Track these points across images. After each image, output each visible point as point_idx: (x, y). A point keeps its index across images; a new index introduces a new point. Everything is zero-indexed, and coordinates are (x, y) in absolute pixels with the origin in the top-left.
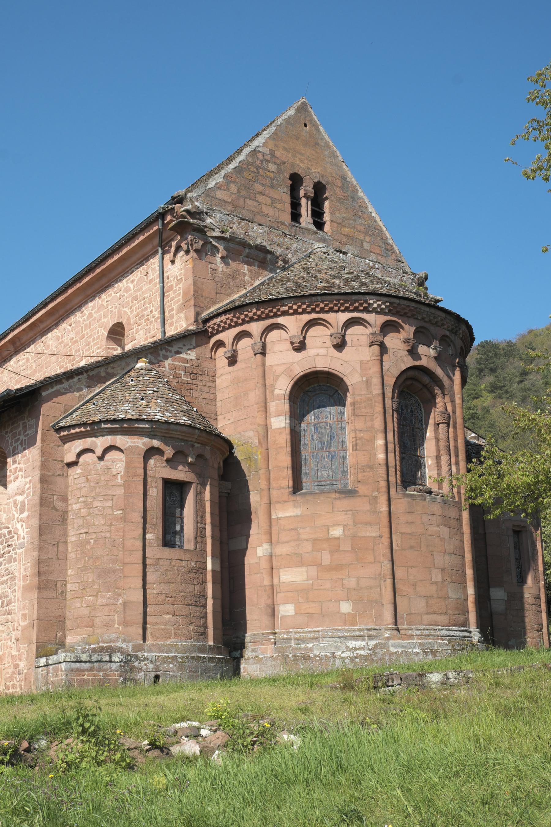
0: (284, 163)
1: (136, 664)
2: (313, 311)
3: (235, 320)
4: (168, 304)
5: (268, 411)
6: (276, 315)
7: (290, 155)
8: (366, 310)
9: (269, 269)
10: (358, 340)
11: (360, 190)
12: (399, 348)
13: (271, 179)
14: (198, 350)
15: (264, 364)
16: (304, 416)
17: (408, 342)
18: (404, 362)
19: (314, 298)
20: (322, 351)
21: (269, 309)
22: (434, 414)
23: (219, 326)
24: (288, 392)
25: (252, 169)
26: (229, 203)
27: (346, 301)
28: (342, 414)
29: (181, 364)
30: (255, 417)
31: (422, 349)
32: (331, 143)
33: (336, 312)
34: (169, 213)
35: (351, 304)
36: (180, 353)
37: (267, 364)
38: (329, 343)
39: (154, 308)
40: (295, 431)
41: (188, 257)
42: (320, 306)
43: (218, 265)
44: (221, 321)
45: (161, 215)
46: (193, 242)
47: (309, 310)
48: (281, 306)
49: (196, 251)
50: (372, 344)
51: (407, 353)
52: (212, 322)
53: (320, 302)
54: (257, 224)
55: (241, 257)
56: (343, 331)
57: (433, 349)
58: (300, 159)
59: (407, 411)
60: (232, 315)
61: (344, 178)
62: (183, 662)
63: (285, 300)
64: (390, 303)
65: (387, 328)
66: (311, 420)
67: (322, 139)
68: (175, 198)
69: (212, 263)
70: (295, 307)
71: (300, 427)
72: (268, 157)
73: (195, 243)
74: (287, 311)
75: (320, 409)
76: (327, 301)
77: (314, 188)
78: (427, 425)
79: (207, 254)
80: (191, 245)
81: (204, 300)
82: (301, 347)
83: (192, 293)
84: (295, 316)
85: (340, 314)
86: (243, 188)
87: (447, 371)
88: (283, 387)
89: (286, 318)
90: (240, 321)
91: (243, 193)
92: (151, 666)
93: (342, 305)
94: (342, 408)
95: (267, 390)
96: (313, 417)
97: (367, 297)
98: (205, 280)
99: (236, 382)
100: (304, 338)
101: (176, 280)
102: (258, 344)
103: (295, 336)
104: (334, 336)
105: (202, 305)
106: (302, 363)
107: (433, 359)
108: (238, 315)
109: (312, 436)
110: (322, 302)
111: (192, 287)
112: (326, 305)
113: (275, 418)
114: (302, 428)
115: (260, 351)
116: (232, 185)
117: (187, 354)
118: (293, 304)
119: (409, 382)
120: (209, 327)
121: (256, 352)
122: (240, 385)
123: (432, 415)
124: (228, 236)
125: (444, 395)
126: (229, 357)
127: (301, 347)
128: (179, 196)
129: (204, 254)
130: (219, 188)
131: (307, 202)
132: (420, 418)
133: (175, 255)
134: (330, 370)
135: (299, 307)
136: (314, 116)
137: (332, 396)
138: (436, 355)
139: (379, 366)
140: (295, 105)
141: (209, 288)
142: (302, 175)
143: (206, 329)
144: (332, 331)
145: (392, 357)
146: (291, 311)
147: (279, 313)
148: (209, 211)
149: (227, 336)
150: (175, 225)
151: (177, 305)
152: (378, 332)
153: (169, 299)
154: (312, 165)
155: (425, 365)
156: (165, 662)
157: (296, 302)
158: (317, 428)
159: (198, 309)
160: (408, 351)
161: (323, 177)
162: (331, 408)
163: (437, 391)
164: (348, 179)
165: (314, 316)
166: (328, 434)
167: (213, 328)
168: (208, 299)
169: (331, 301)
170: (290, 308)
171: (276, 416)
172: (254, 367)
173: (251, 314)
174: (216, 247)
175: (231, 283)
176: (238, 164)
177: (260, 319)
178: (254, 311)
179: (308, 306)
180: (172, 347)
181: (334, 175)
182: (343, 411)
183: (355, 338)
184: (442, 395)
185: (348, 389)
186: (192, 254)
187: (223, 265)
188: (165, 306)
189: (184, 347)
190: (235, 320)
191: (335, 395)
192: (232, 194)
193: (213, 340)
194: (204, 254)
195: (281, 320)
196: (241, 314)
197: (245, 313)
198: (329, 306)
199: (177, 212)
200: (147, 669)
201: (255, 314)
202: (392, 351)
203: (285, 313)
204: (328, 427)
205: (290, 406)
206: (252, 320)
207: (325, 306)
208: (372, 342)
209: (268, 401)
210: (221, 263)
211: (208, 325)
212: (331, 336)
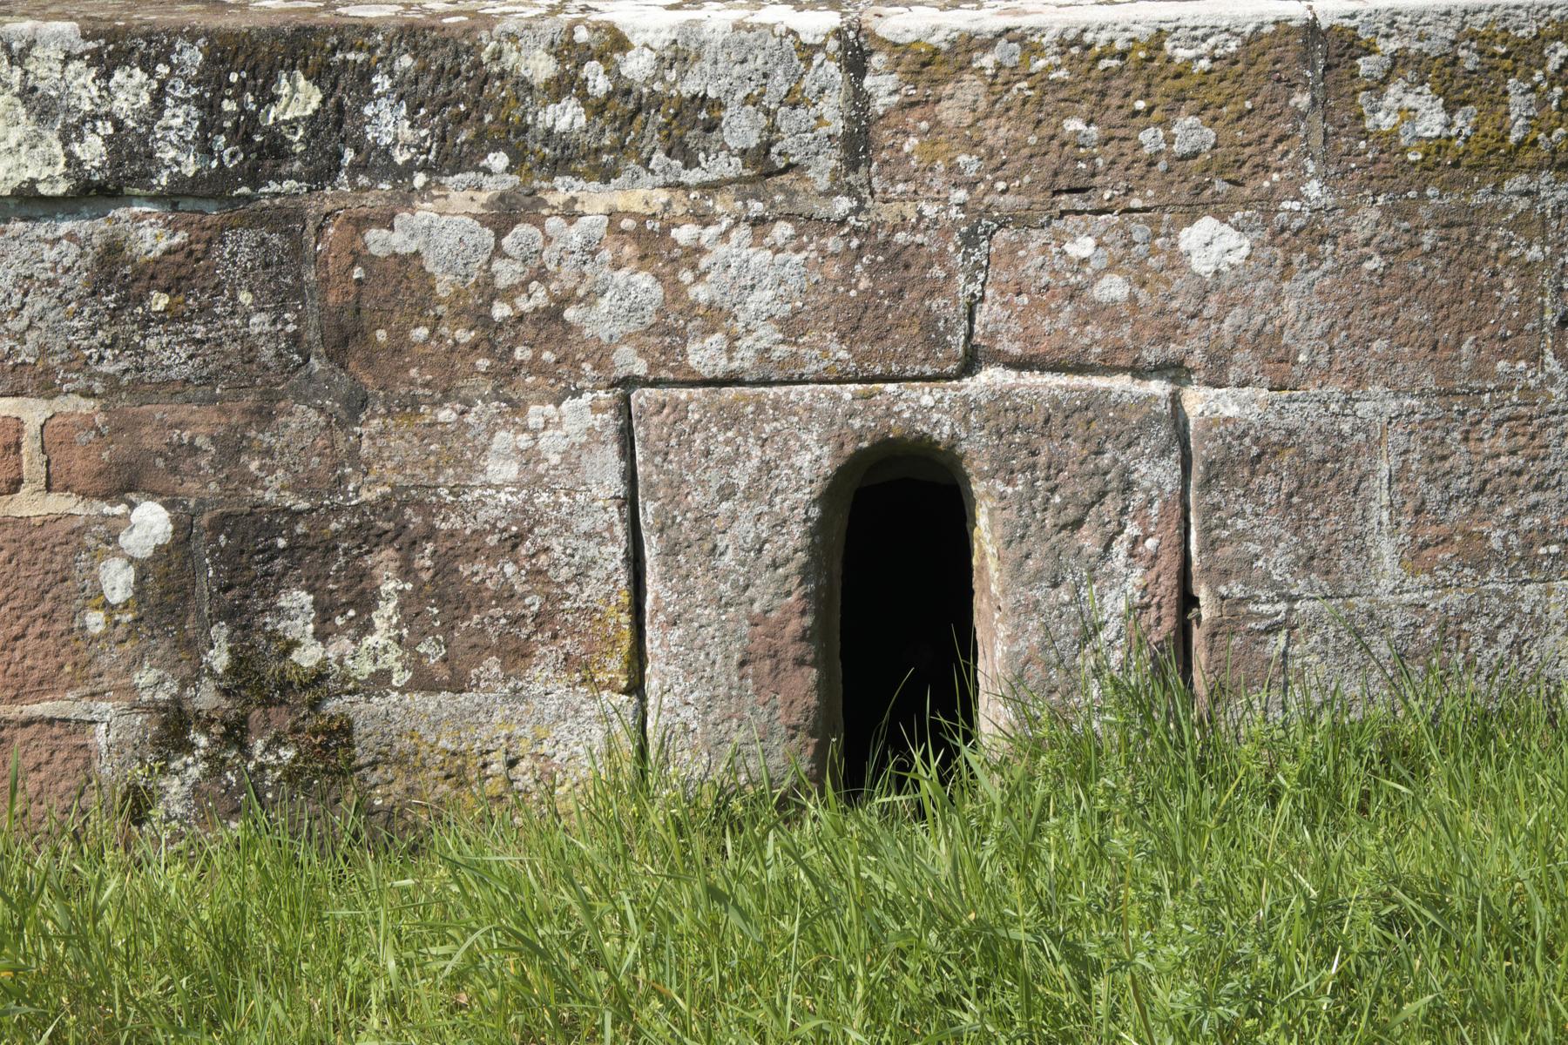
1: (441, 227)
62: (1497, 157)
92: (755, 273)
156: (1070, 187)
200: (669, 329)
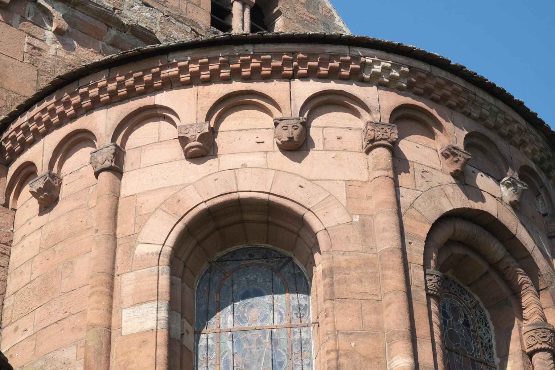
2: (236, 75)
3: (60, 109)
5: (115, 294)
6: (150, 90)
8: (356, 77)
10: (339, 138)
12: (434, 166)
15: (116, 195)
16: (208, 315)
17: (455, 155)
18: (446, 196)
19: (237, 50)
20: (256, 159)
21: (135, 75)
22: (520, 331)
23: (26, 130)
24: (168, 249)
27: (311, 56)
28: (301, 310)
30: (83, 313)
31: (483, 182)
33: (290, 78)
35: (323, 63)
37: (124, 192)
38: (271, 143)
40: (182, 346)
42: (252, 65)
43: (48, 43)
44: (31, 120)
47: (225, 73)
48: (162, 68)
50: (371, 145)
51: (453, 181)
53: (253, 56)
55: (101, 43)
56: (306, 116)
57: (508, 186)
59: (456, 319)
60: (54, 100)
63: (171, 56)
64: (410, 68)
65: (405, 119)
66: (226, 324)
69: (33, 37)
70: (194, 68)
71: (198, 340)
74: (177, 77)
75: (249, 300)
76: (267, 53)
78: (504, 357)
79: (23, 19)
81: (5, 95)
82: (202, 149)
84: (194, 88)
85: (297, 83)
87: (540, 242)
88: (157, 236)
89: (174, 93)
90: (70, 111)
93: (303, 62)
94: (301, 296)
95: (119, 250)
96: (230, 318)
97: (359, 51)
98: (12, 61)
99: (51, 245)
100: (214, 131)
103: (191, 125)
104: (282, 124)
106: (203, 186)
107: (510, 208)
108: (66, 96)
109: (227, 361)
110: (256, 56)
112: (266, 63)
113: (131, 309)
114: (202, 343)
115: (108, 164)
118: (190, 62)
119: (459, 251)
120: (6, 140)
121: (99, 167)
122: (59, 247)
123: (515, 333)
125: (538, 291)
126: (39, 190)
127: (202, 149)
129: (17, 18)
132: (485, 341)
134: (272, 198)
135: (204, 67)
137: (278, 271)
138: (515, 198)
139: (391, 191)
144: (277, 114)
145: (420, 181)
146: (185, 78)
147: (157, 84)
152: (387, 122)
155: (494, 212)
157: (198, 56)
158: (239, 341)
160: (456, 175)
162: (276, 296)
163: (522, 278)
165: (237, 86)
166: (266, 357)
167: (14, 139)
168: (13, 95)
169: (277, 55)
170: (183, 70)
171: (134, 305)
172: (92, 203)
173: (94, 92)
174: (46, 12)
177: (115, 100)
179: (224, 65)
182: (303, 303)
183: (331, 135)
184: (533, 289)
185: (317, 244)
187: (59, 46)
190: (60, 109)
191: (286, 269)
194: (17, 18)
195: (161, 99)
196: (73, 94)
197: (81, 91)
198: (273, 64)
201: (103, 89)
202: (418, 168)
203: (171, 84)
204: (268, 340)
205: (172, 284)
206: (97, 104)
207: (262, 65)
208: (372, 141)
209: (118, 272)
210: (54, 42)
212: (276, 124)
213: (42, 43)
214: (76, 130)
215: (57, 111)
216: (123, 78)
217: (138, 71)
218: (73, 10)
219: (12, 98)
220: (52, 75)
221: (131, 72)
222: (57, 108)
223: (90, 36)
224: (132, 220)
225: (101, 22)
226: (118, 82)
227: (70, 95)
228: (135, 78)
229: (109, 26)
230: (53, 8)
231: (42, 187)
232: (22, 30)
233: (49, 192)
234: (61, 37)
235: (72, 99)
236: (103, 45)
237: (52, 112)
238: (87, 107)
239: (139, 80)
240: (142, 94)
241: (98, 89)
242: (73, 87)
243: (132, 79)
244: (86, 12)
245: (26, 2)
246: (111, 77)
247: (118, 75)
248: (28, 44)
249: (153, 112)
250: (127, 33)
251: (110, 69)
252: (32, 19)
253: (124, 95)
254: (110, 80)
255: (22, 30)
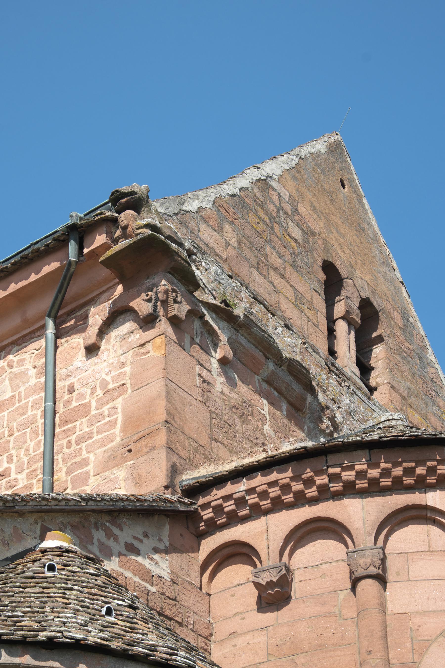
0: (313, 234)
3: (297, 487)
4: (65, 450)
7: (322, 224)
9: (306, 428)
11: (430, 351)
13: (294, 252)
14: (175, 558)
23: (241, 502)
25: (261, 213)
26: (222, 259)
29: (137, 579)
32: (382, 239)
34: (104, 228)
36: (138, 553)
37: (390, 608)
39: (13, 466)
41: (150, 334)
43: (214, 374)
45: (79, 232)
46: (171, 299)
49: (175, 321)
52: (217, 494)
54: (282, 323)
55: (257, 378)
58: (337, 240)
60: (290, 473)
61: (405, 316)
67: (369, 224)
68: (124, 195)
72: (288, 208)
73: (175, 301)
77: (360, 308)
80: (165, 303)
81: (187, 443)
83: (162, 416)
86: (248, 244)
90: (312, 492)
91: (247, 252)
98: (188, 398)
101: (99, 392)
102: (369, 552)
105: (184, 453)
108: (308, 473)
111: (163, 402)
115: (373, 570)
116: (227, 227)
117: (152, 559)
120: (205, 506)
124: (241, 315)
128: (133, 193)
130: (205, 220)
131: (349, 334)
133: (103, 331)
136: (355, 177)
140: (326, 139)
141: (196, 420)
142: (343, 272)
143: (196, 511)
147: (431, 480)
148: (195, 251)
149: (266, 532)
150: (129, 247)
151: (100, 451)
153: (73, 438)
154: (356, 263)
159: (175, 459)
161: (373, 293)
164: (411, 320)
173: (349, 475)
174: (211, 332)
175: (238, 428)
176: (237, 191)
177: (375, 489)
178: (361, 466)
180: (121, 530)
181: (390, 300)
186: (163, 325)
188: (58, 457)
189: (145, 540)
190: (297, 487)
192: (228, 245)
193: (209, 544)
196: (319, 472)
197: (331, 470)
199: (125, 228)
201: (361, 475)
206: (350, 490)
211: (202, 501)
213: (209, 374)
214: (319, 517)
215: (294, 489)
216: (389, 465)
217: (410, 461)
218: (236, 332)
219: (193, 448)
220: (221, 419)
221: (400, 460)
222: (293, 484)
223: (248, 367)
224: (409, 645)
225: (260, 351)
226: (382, 470)
227: (314, 472)
228: (405, 468)
229: (267, 358)
230: (219, 329)
231: (275, 580)
232: (193, 356)
233: (282, 587)
234: (224, 367)
235: (316, 478)
236: (259, 380)
237: (286, 488)
238: (337, 491)
239: (409, 472)
240: (409, 489)
241: (353, 473)
242: (319, 463)
243: (401, 468)
244: (248, 337)
245: (194, 317)
246: (373, 461)
247: (383, 460)
248: (200, 375)
249: (423, 513)
250: (282, 368)
251: (370, 450)
252: (200, 342)
253: (388, 486)
254: (373, 465)
255: (193, 356)
